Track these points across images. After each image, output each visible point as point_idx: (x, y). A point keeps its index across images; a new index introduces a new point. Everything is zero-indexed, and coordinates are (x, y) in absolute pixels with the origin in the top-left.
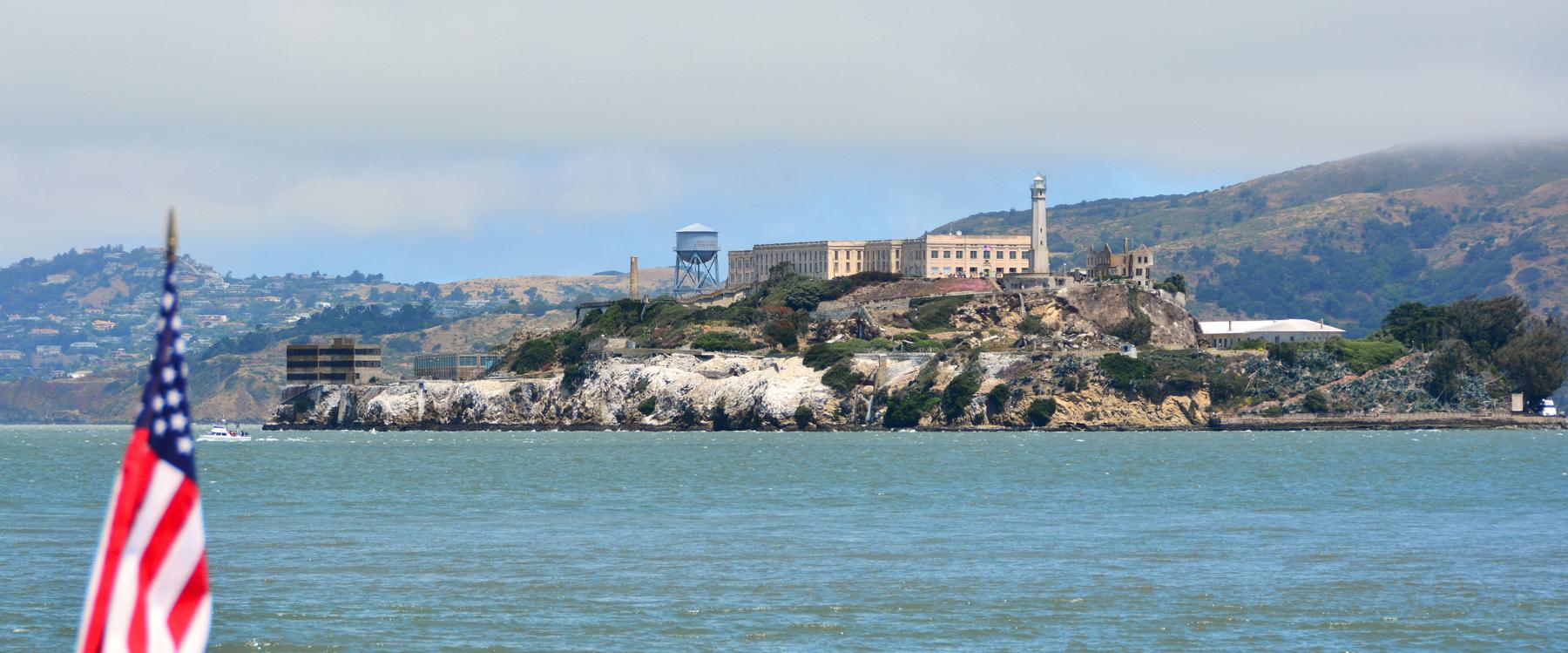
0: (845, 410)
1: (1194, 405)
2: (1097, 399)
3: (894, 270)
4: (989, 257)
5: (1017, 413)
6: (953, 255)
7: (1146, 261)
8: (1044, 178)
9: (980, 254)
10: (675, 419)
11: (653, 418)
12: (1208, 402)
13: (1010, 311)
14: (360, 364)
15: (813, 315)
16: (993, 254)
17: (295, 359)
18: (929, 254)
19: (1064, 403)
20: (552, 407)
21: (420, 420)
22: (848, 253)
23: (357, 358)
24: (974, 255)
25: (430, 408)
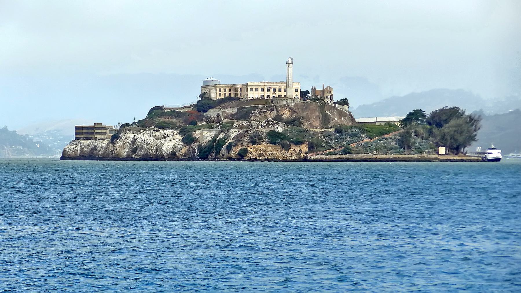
1: (301, 151)
3: (239, 96)
5: (234, 154)
6: (260, 90)
7: (330, 93)
8: (292, 59)
9: (271, 90)
11: (136, 155)
13: (271, 113)
14: (97, 133)
15: (205, 114)
16: (277, 90)
17: (78, 131)
18: (249, 90)
19: (251, 150)
21: (78, 156)
23: (96, 131)
25: (82, 150)
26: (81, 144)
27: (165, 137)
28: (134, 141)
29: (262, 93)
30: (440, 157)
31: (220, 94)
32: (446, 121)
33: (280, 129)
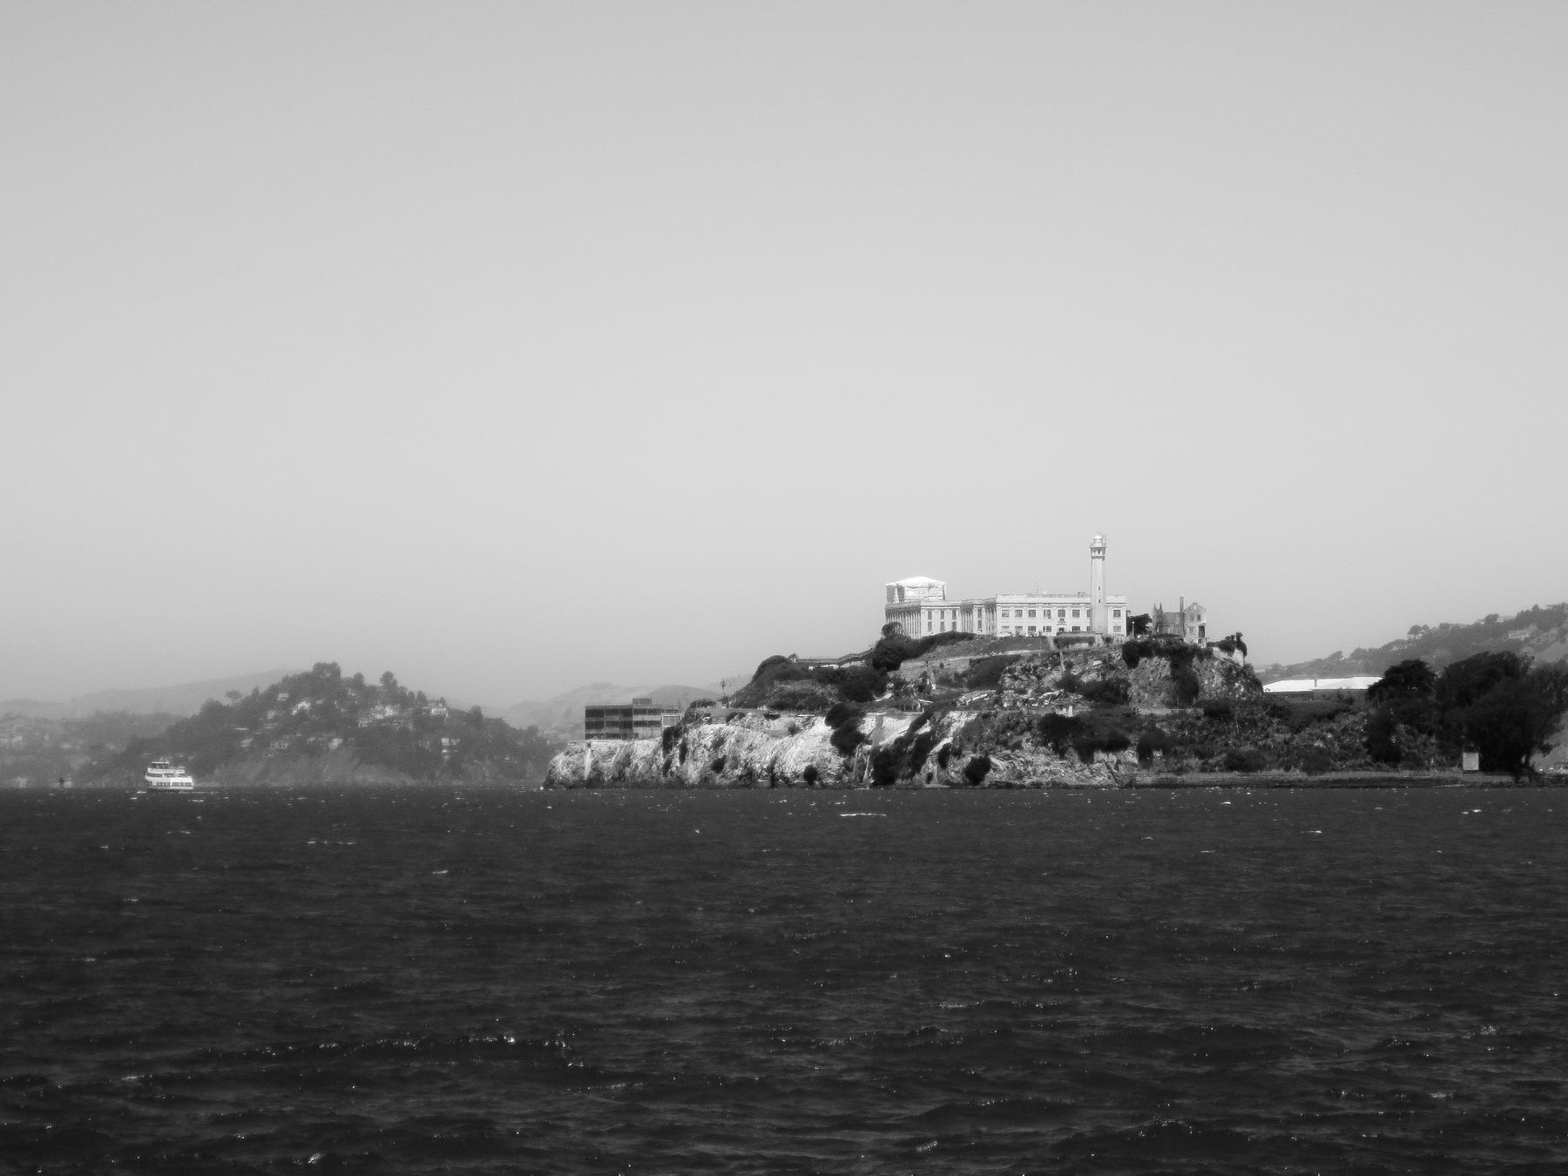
0: (847, 768)
2: (1029, 758)
3: (976, 631)
4: (1064, 615)
5: (956, 772)
6: (1025, 614)
7: (1199, 618)
9: (1054, 613)
10: (740, 777)
12: (1136, 761)
14: (642, 724)
15: (891, 675)
16: (1069, 613)
17: (594, 720)
20: (654, 766)
22: (942, 613)
24: (1048, 614)
26: (592, 751)
27: (793, 730)
28: (719, 743)
29: (1032, 622)
30: (1466, 778)
31: (930, 624)
32: (1483, 686)
33: (1069, 713)
